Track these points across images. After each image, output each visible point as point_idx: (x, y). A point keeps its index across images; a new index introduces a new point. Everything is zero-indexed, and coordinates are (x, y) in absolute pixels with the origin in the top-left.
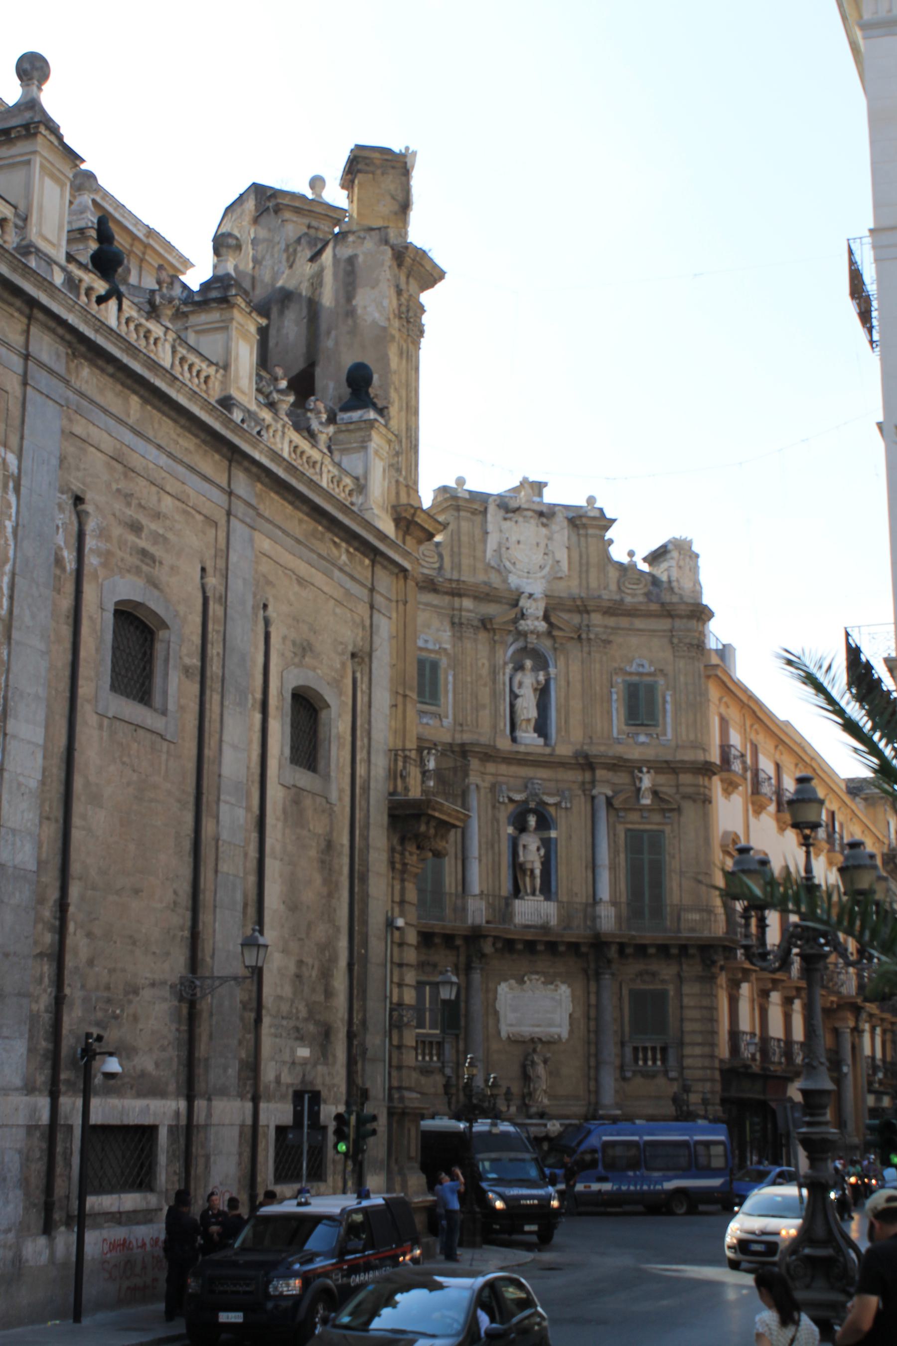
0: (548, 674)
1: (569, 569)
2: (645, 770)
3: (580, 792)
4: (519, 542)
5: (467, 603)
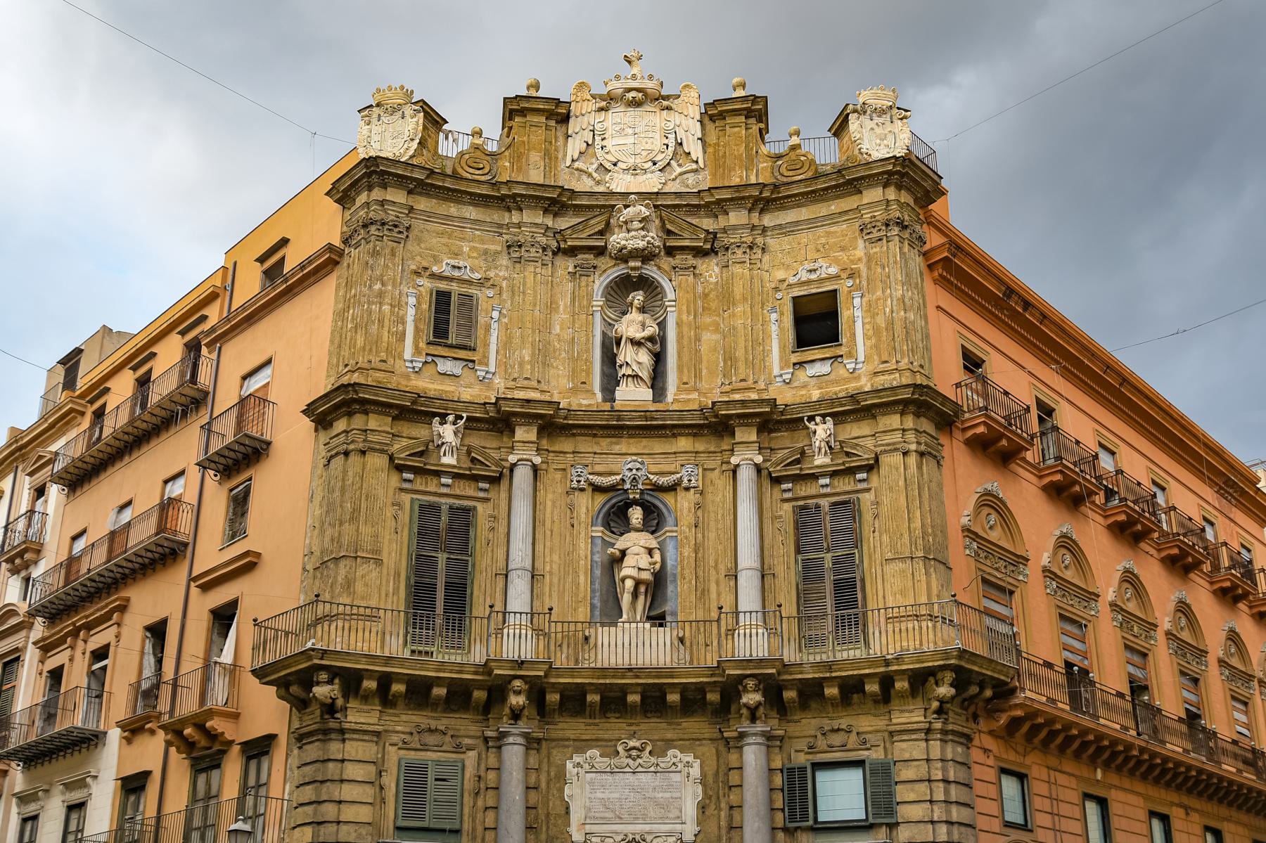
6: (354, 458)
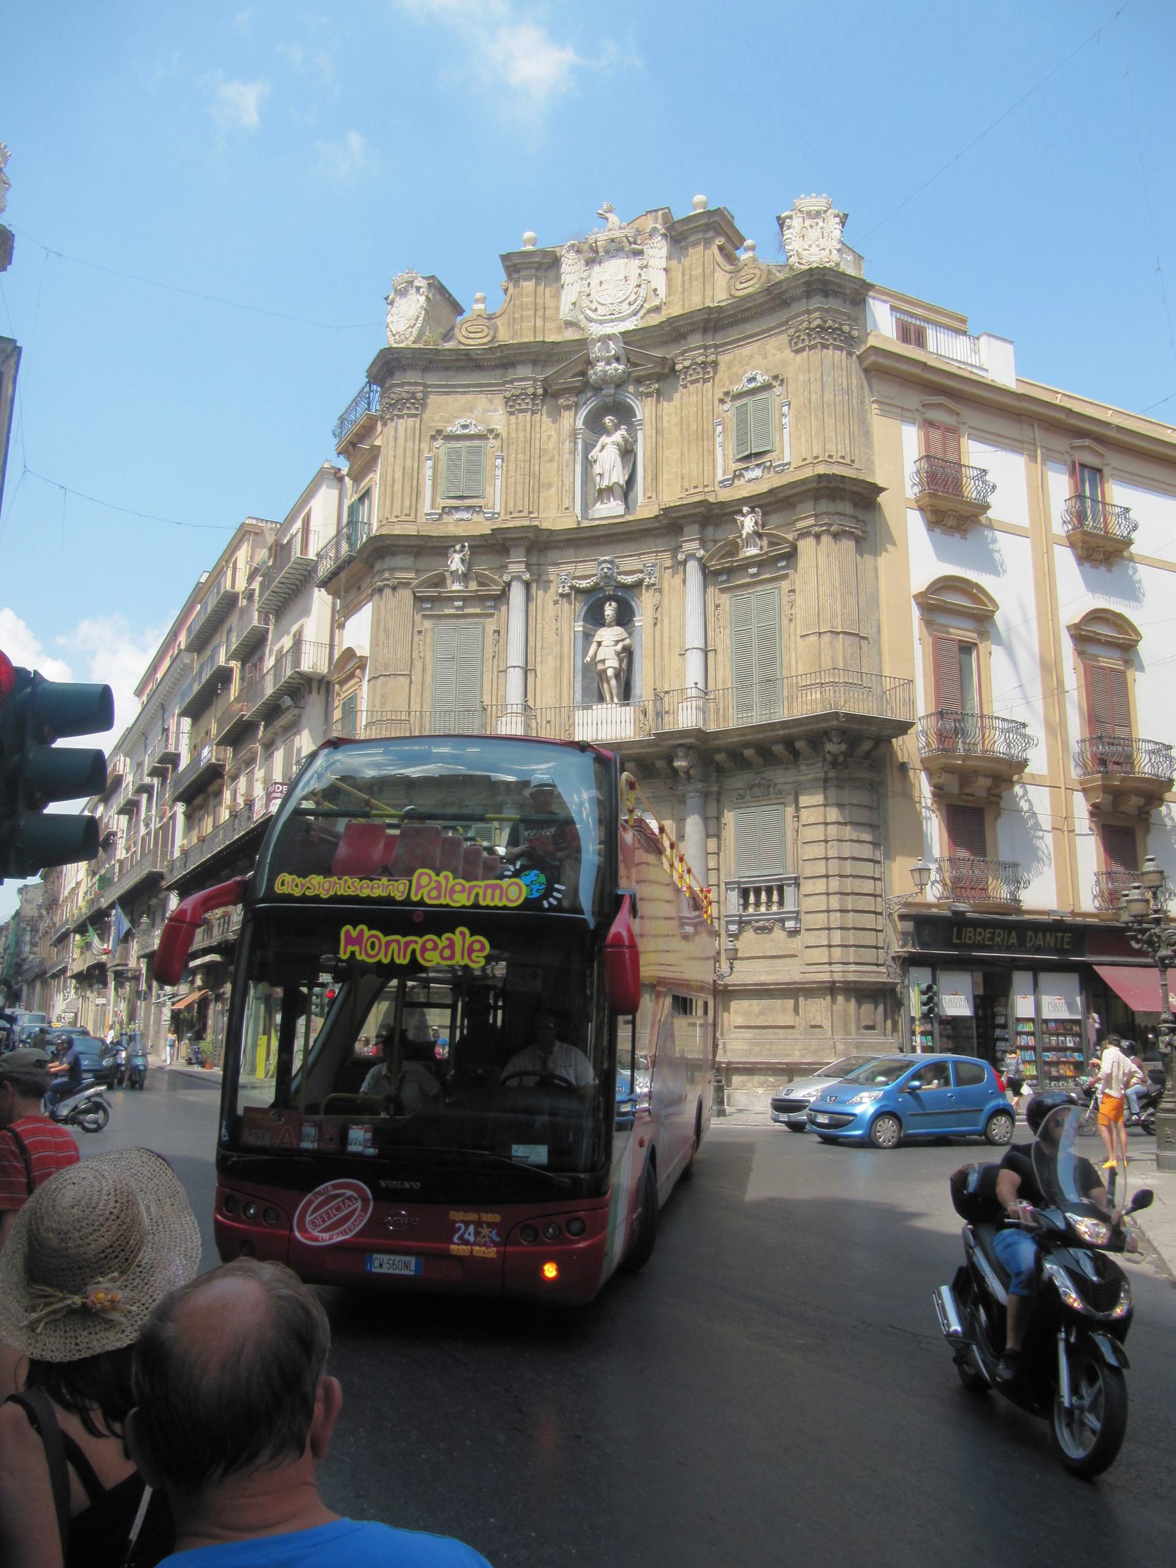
2: (745, 509)
5: (524, 371)
6: (388, 592)
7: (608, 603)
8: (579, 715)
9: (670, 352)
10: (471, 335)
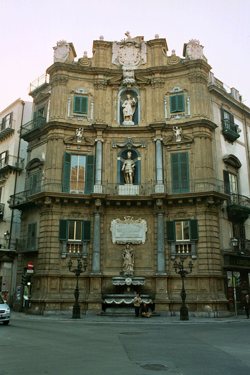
0: (137, 99)
1: (147, 61)
2: (177, 128)
3: (151, 141)
4: (125, 54)
5: (101, 77)
7: (129, 152)
8: (120, 187)
9: (149, 77)
10: (84, 63)
